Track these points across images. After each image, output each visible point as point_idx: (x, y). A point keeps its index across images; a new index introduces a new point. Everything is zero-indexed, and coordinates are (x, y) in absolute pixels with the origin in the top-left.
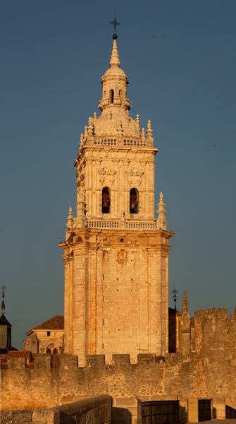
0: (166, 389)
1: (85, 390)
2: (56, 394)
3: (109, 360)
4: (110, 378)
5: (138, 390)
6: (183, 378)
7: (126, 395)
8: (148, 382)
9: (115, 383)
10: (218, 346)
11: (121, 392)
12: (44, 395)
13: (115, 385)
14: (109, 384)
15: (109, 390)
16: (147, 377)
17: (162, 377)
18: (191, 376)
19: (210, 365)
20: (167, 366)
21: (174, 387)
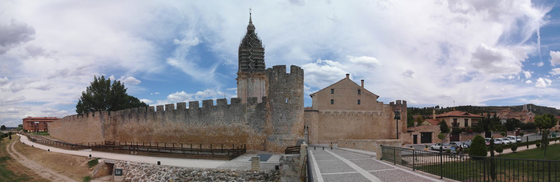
0: (248, 120)
1: (202, 121)
2: (188, 123)
3: (215, 104)
4: (215, 113)
5: (231, 120)
6: (258, 113)
7: (224, 123)
8: (238, 115)
9: (218, 116)
10: (279, 91)
11: (221, 121)
12: (182, 124)
13: (218, 118)
14: (215, 117)
15: (215, 120)
16: (237, 112)
17: (245, 112)
18: (263, 111)
19: (274, 104)
20: (248, 105)
21: (252, 118)
